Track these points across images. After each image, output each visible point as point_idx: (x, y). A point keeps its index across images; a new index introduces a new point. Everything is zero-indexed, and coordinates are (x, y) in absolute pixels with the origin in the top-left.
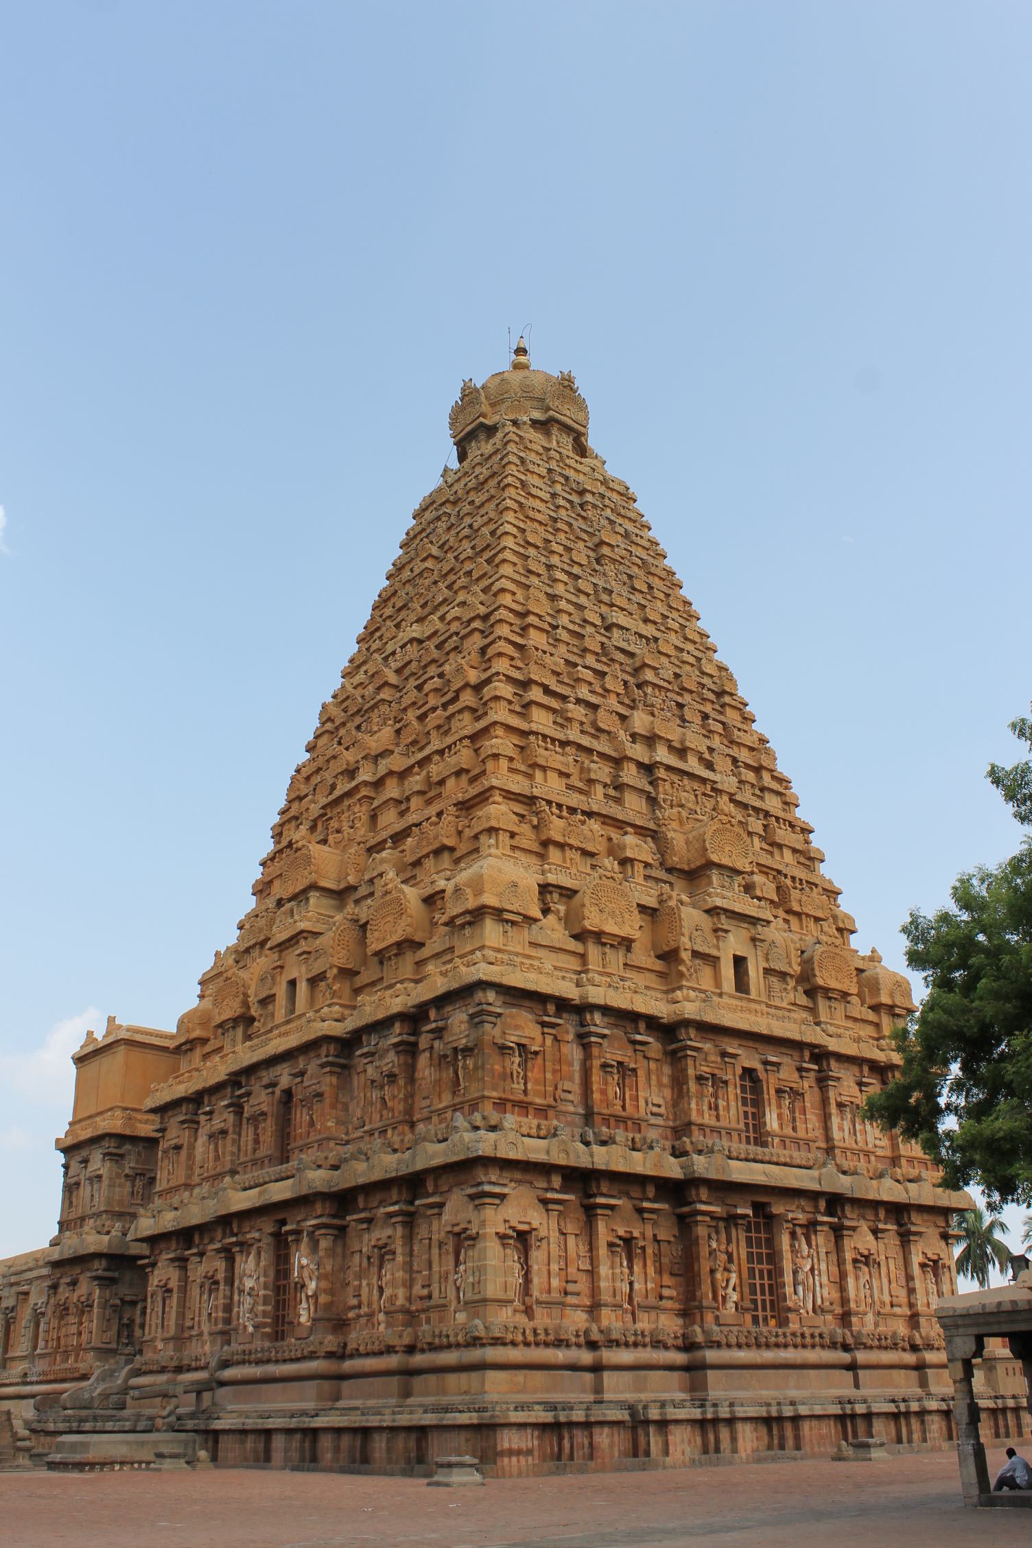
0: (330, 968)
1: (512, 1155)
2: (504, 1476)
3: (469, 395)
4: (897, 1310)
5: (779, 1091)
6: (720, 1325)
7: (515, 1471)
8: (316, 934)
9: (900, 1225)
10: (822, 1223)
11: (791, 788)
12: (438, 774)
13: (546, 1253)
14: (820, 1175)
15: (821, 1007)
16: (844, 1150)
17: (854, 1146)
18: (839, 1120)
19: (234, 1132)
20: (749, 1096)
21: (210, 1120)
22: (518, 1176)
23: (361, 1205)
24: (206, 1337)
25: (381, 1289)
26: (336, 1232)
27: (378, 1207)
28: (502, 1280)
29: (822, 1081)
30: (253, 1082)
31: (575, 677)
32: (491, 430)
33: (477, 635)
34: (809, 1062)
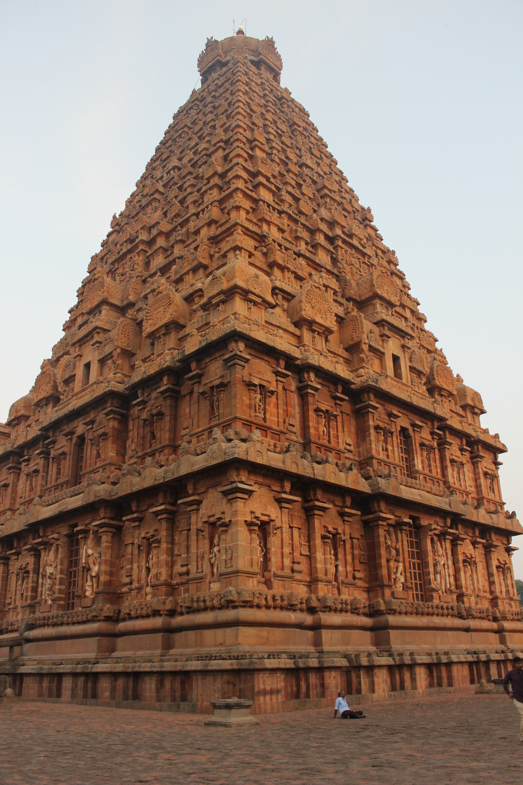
0: (115, 349)
1: (259, 460)
2: (260, 713)
3: (211, 44)
5: (422, 445)
6: (395, 598)
7: (269, 708)
8: (106, 331)
13: (280, 539)
14: (450, 501)
19: (43, 471)
21: (28, 465)
22: (260, 480)
23: (134, 509)
24: (19, 609)
25: (148, 570)
27: (147, 509)
28: (249, 557)
29: (442, 444)
30: (57, 434)
31: (284, 181)
33: (221, 151)
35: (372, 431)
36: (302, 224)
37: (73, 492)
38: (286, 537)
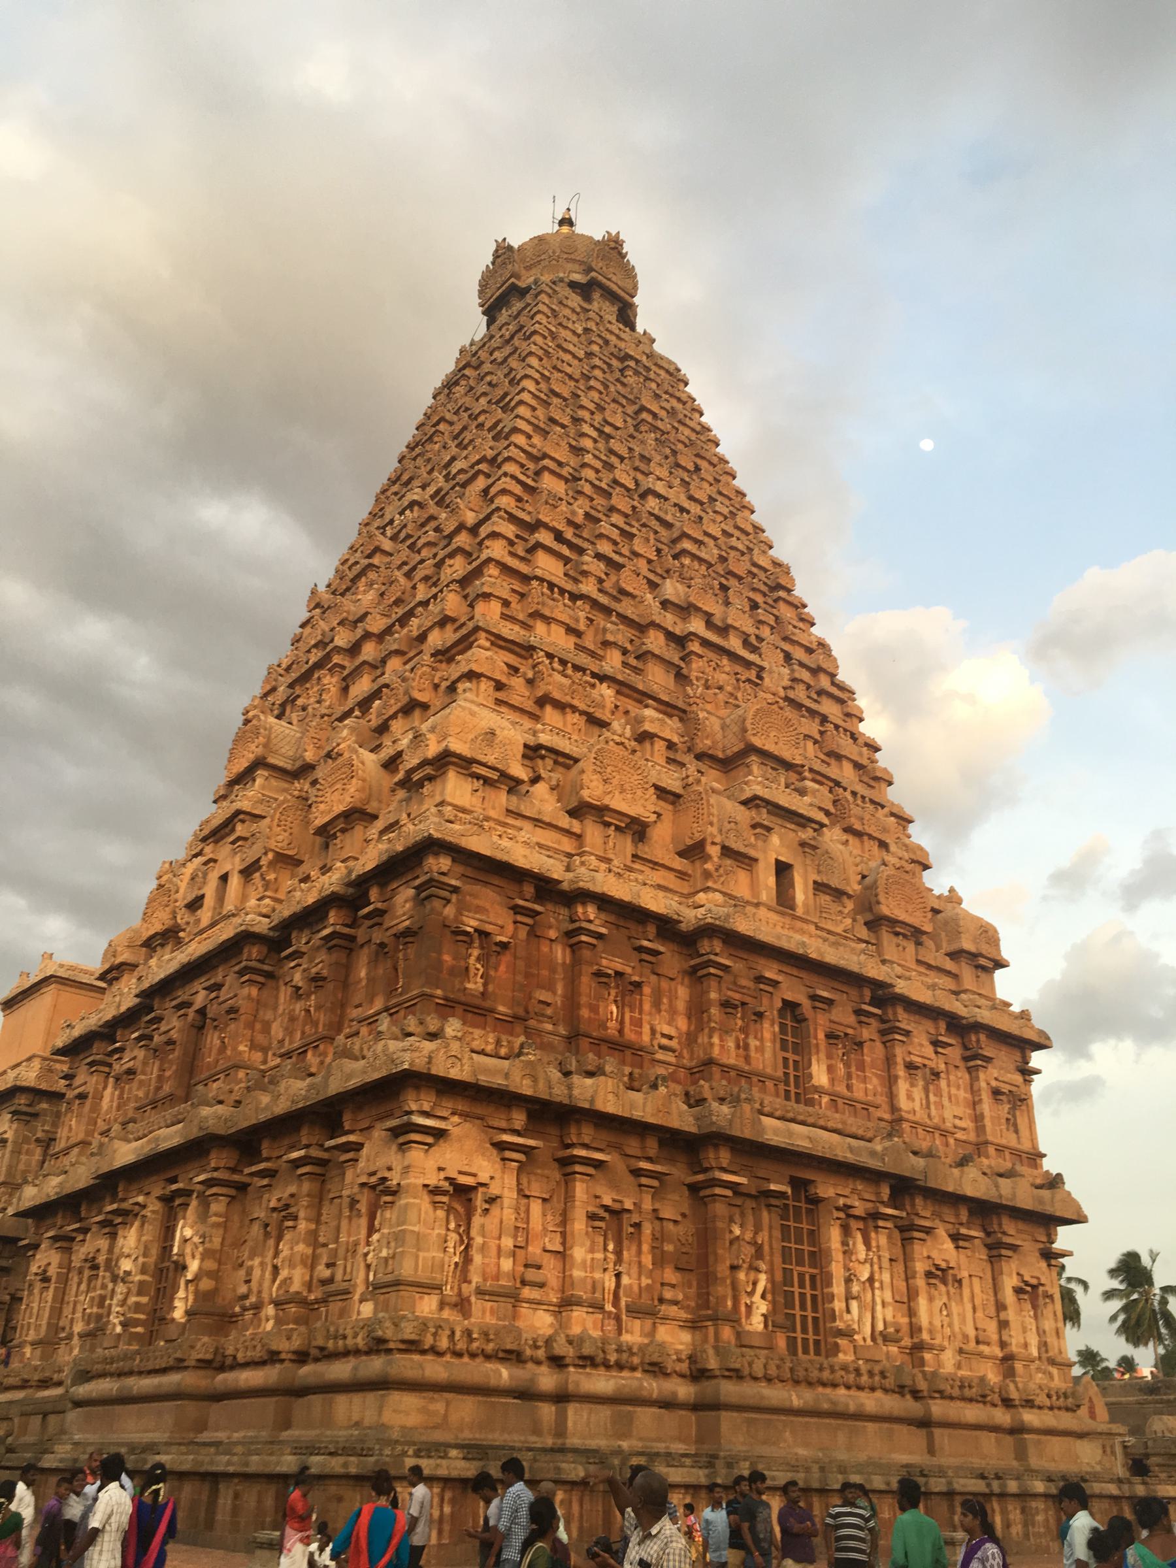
0: (266, 854)
1: (454, 1074)
4: (982, 1348)
5: (829, 1036)
9: (988, 1234)
10: (886, 1217)
11: (854, 700)
12: (419, 627)
13: (496, 1221)
14: (885, 1149)
15: (885, 943)
16: (915, 1125)
17: (929, 1122)
18: (907, 1086)
20: (789, 1038)
21: (120, 1058)
23: (265, 1154)
25: (276, 1269)
26: (232, 1192)
29: (888, 1032)
31: (597, 532)
32: (523, 292)
34: (870, 1004)
35: (714, 1011)
36: (619, 615)
37: (175, 1116)
38: (509, 1215)
